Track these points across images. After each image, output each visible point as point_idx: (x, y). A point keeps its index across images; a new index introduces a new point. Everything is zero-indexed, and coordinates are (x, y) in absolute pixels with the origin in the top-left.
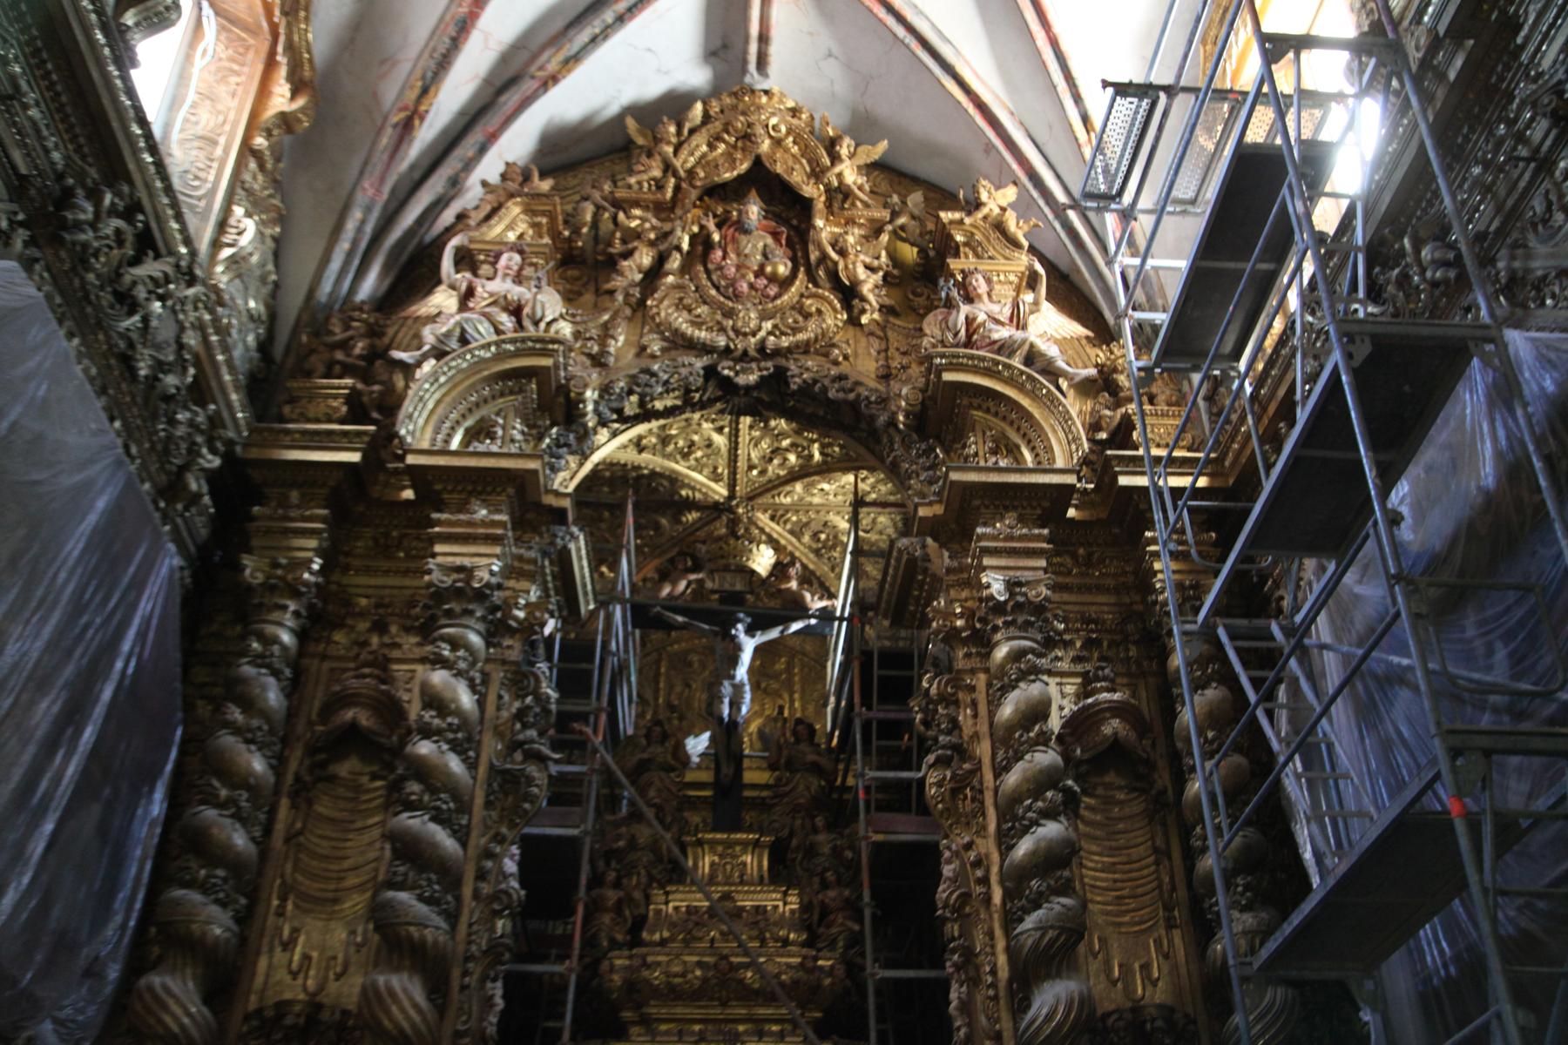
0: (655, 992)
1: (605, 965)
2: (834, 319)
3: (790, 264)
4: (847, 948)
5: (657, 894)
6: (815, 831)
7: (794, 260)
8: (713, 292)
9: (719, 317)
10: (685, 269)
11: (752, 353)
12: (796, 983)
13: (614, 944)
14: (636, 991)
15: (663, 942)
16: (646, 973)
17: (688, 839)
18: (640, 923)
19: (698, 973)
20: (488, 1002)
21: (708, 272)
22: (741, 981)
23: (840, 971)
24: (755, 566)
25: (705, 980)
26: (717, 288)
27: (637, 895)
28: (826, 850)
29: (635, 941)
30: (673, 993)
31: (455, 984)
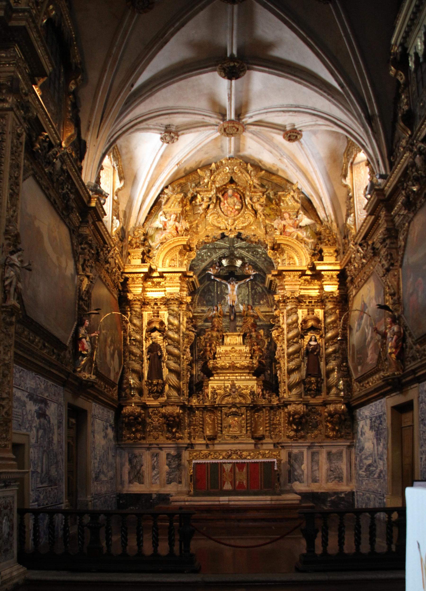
0: (219, 368)
1: (208, 363)
2: (252, 219)
3: (241, 205)
4: (259, 358)
5: (218, 349)
6: (252, 332)
7: (242, 203)
8: (222, 214)
9: (224, 220)
10: (215, 207)
11: (233, 229)
12: (248, 366)
13: (210, 359)
14: (215, 368)
15: (220, 357)
16: (217, 365)
17: (224, 334)
18: (215, 353)
19: (228, 364)
20: (188, 376)
21: (221, 209)
22: (237, 367)
23: (257, 363)
24: (237, 265)
25: (229, 367)
26: (223, 212)
27: (214, 348)
28: (255, 336)
29: (214, 358)
30: (223, 368)
31: (181, 375)
